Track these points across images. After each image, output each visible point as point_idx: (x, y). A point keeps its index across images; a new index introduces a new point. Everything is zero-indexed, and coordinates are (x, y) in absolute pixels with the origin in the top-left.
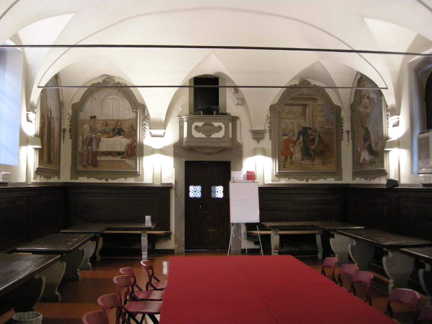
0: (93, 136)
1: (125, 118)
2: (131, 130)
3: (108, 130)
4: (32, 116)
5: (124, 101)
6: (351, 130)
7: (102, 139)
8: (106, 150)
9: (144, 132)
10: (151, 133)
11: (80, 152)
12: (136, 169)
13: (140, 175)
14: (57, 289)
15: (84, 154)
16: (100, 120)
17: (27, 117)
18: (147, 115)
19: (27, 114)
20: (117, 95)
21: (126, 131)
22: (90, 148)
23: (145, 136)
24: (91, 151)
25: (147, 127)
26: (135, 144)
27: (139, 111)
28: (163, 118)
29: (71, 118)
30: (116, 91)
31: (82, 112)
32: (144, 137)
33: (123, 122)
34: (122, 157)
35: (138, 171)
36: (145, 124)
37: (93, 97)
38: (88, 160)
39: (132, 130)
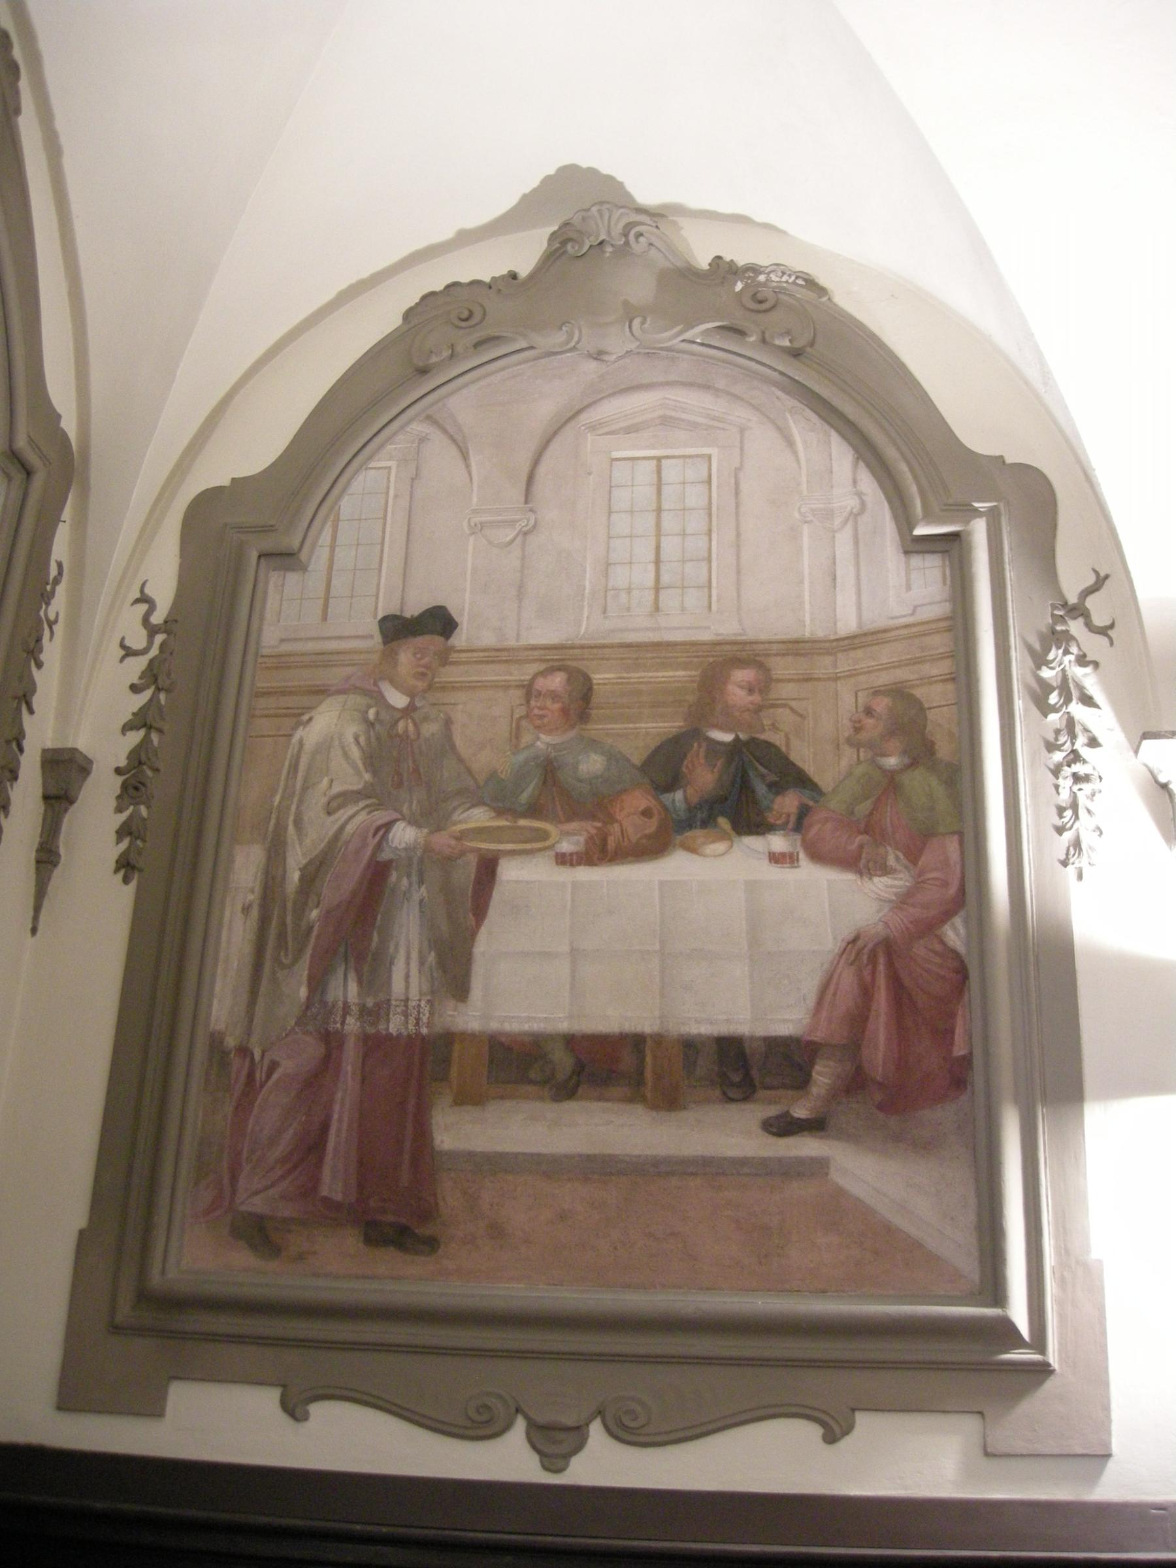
0: (404, 835)
1: (811, 626)
2: (892, 762)
3: (592, 764)
5: (790, 443)
7: (510, 872)
8: (564, 1026)
9: (1066, 783)
11: (216, 1042)
12: (996, 1292)
13: (1050, 1384)
15: (274, 1066)
16: (499, 655)
18: (1091, 580)
20: (706, 387)
21: (825, 779)
22: (353, 988)
23: (1084, 826)
24: (365, 1038)
26: (954, 934)
27: (979, 530)
29: (159, 638)
30: (695, 333)
31: (292, 578)
32: (1077, 844)
33: (781, 667)
34: (773, 1111)
35: (1019, 1313)
37: (429, 418)
39: (913, 764)
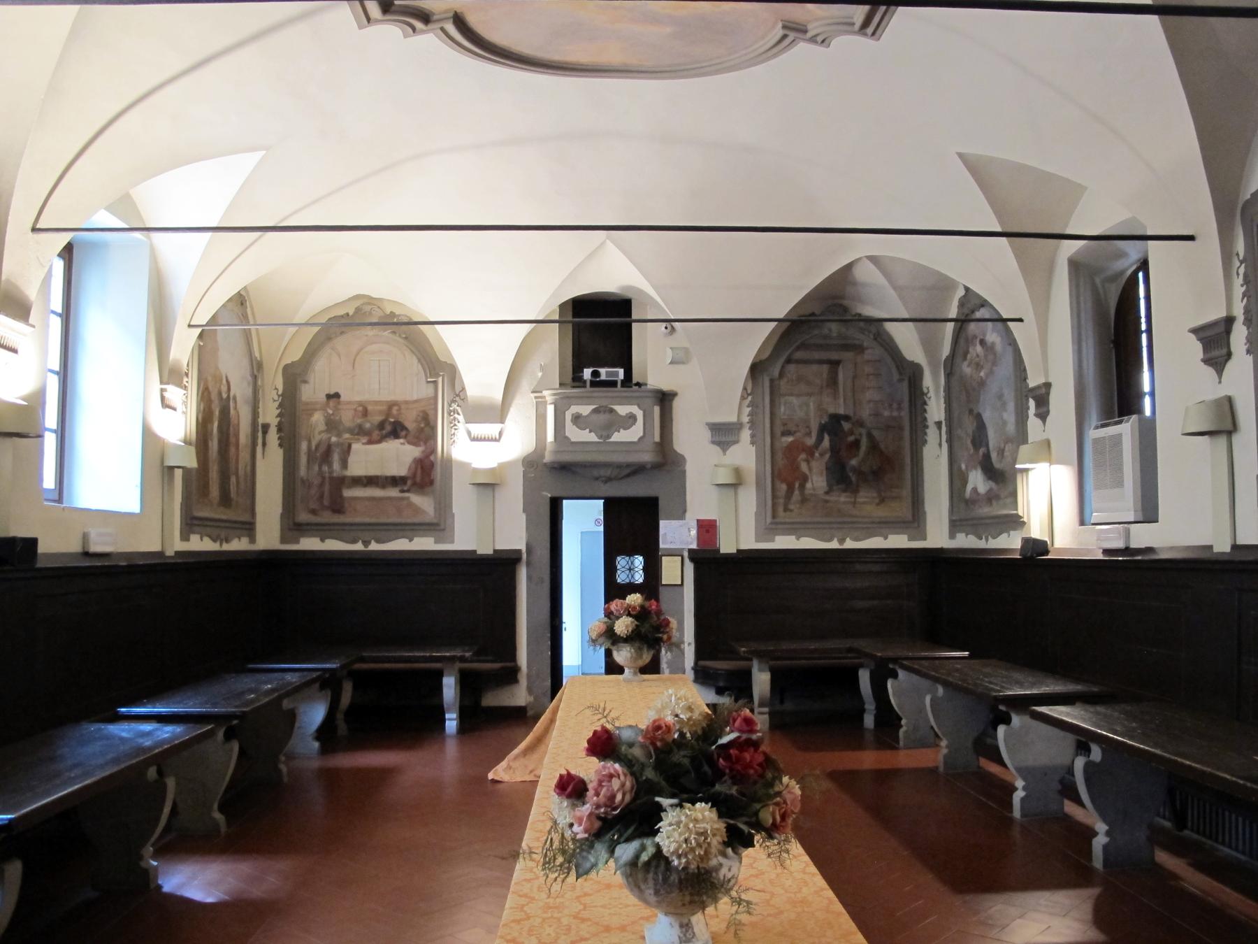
1: (408, 398)
2: (422, 425)
3: (368, 425)
4: (174, 393)
6: (945, 420)
7: (355, 446)
9: (453, 431)
10: (469, 433)
11: (303, 481)
14: (216, 806)
16: (349, 403)
17: (163, 398)
19: (162, 390)
22: (327, 468)
23: (455, 438)
24: (330, 478)
25: (461, 418)
26: (432, 458)
27: (440, 379)
28: (498, 396)
31: (307, 385)
32: (454, 441)
33: (403, 406)
36: (455, 411)
37: (332, 349)
38: (322, 496)
